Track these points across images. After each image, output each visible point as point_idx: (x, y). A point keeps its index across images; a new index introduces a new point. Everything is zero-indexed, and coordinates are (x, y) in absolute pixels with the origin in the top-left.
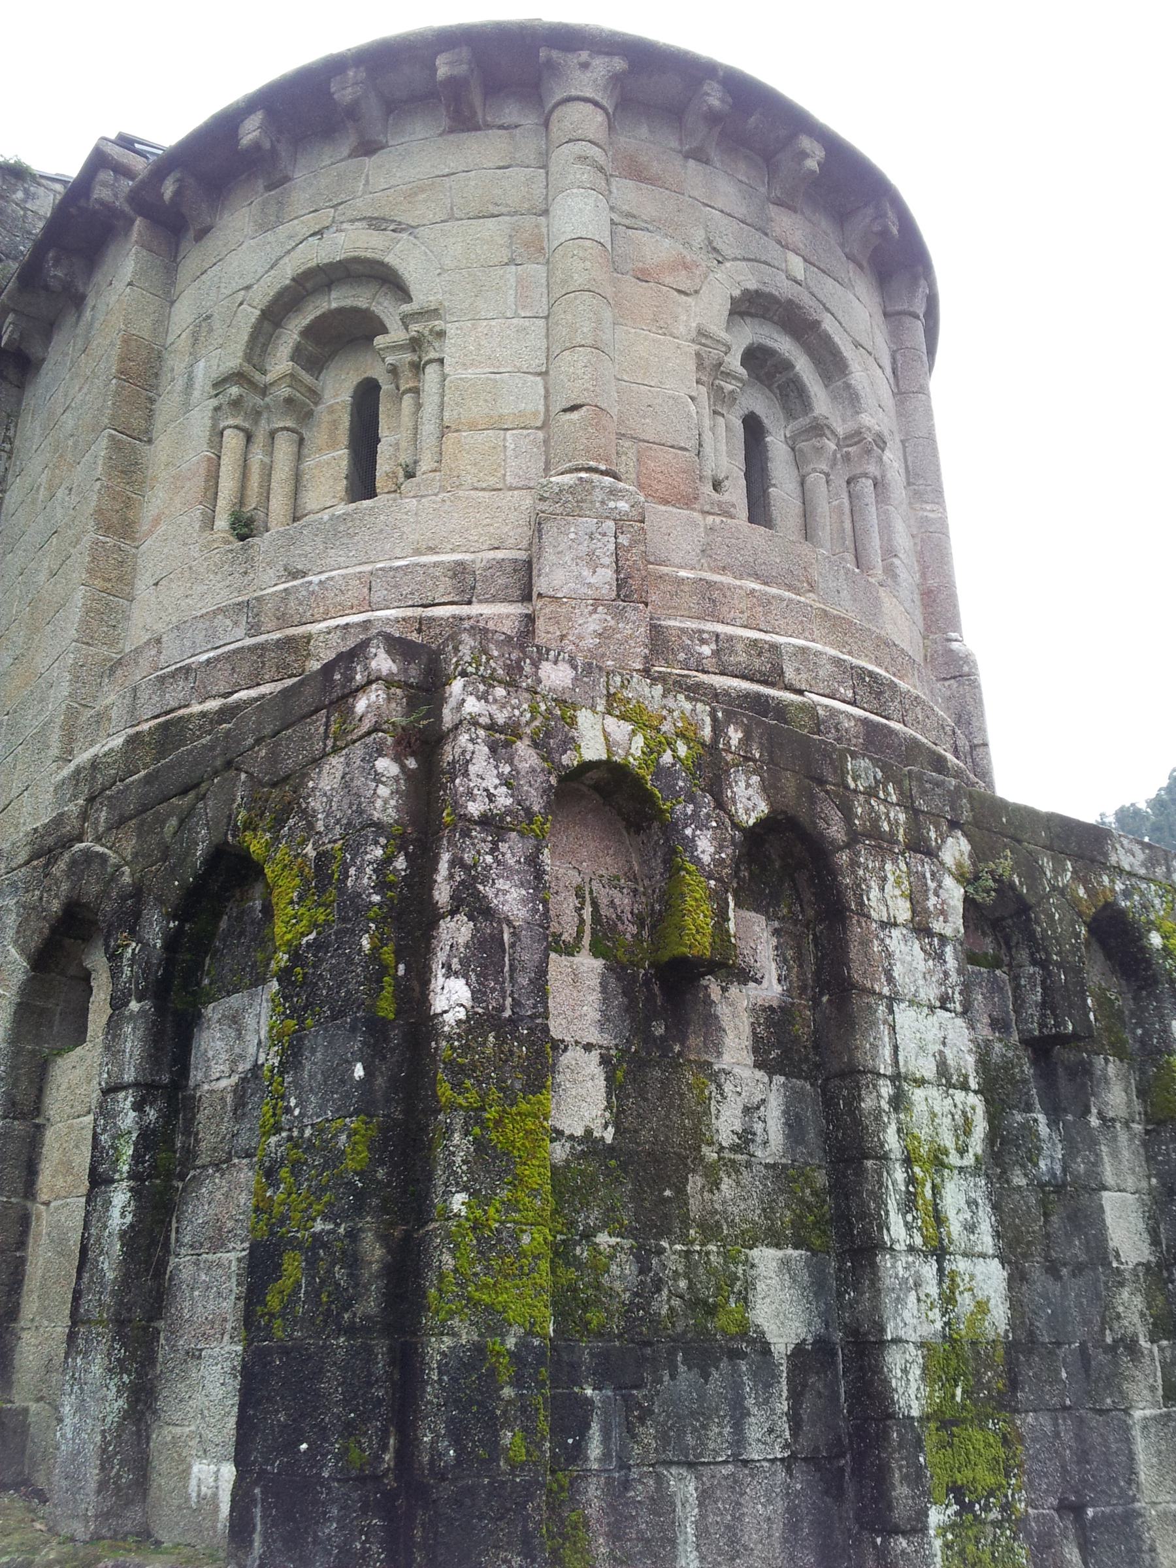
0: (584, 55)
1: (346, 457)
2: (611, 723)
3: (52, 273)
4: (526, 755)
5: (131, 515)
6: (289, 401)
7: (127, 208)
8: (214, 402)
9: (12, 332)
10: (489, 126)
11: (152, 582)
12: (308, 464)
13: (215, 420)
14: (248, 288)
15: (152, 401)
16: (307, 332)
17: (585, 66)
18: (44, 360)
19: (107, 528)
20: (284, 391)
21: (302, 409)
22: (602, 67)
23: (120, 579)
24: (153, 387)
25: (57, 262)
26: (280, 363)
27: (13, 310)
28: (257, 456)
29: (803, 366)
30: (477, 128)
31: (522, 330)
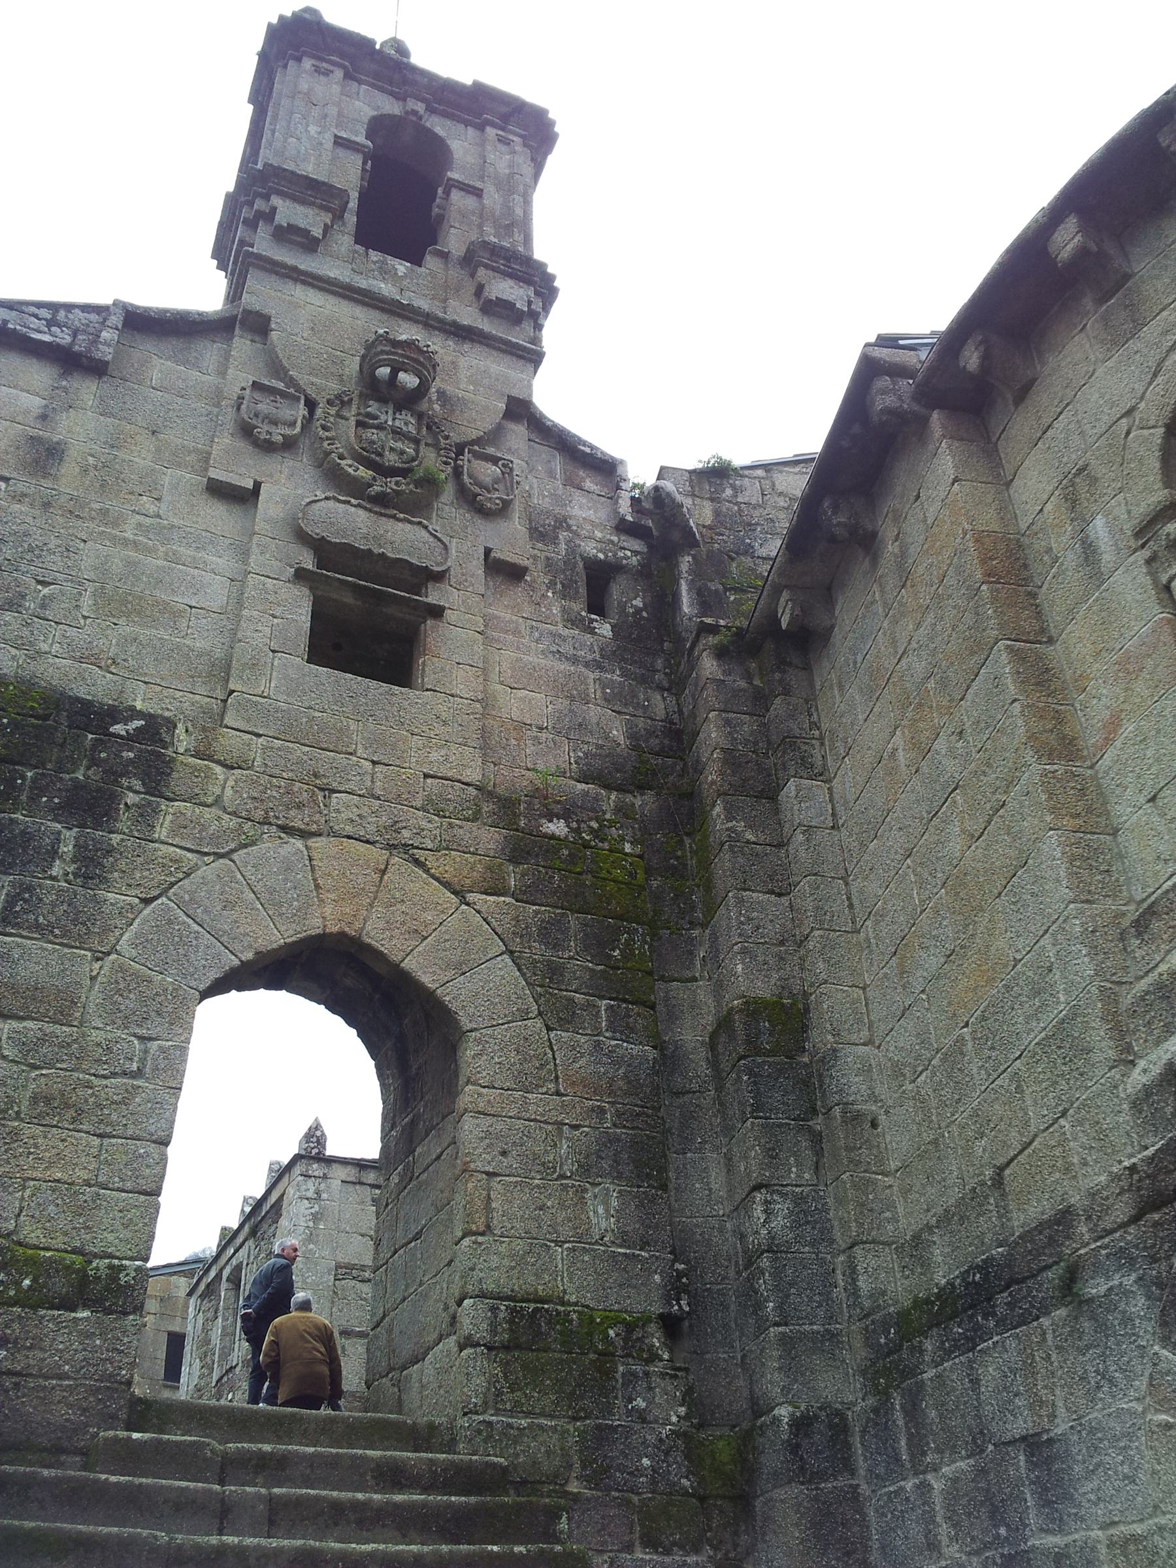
3: (835, 522)
5: (1067, 731)
7: (916, 408)
8: (1146, 553)
9: (793, 609)
11: (1142, 800)
14: (1129, 412)
15: (1034, 595)
18: (833, 627)
19: (1048, 754)
23: (1089, 810)
24: (1027, 581)
25: (836, 508)
27: (786, 587)
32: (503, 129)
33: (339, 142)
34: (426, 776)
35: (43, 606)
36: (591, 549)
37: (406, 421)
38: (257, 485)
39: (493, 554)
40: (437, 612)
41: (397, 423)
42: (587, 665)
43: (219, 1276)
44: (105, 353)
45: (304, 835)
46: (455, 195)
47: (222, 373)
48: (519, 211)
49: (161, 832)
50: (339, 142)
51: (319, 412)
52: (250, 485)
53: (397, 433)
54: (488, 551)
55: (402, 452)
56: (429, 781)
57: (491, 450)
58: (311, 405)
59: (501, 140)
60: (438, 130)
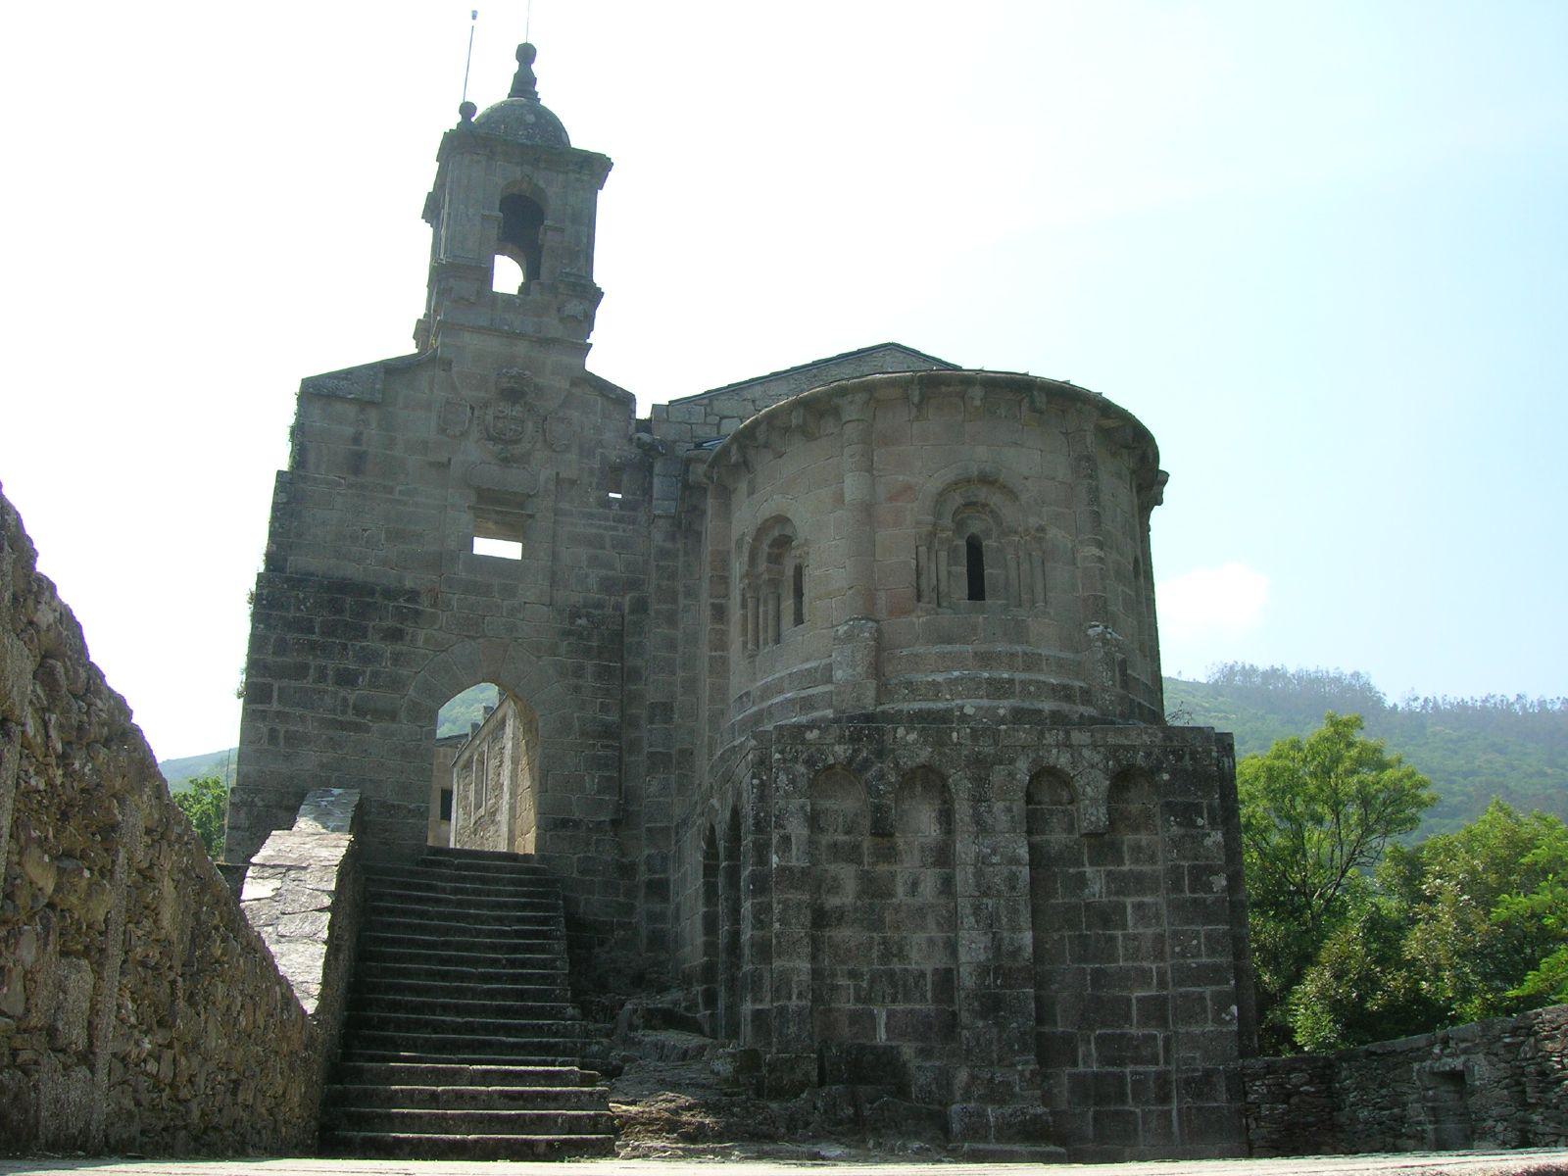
0: (850, 397)
1: (793, 606)
2: (837, 748)
4: (801, 769)
6: (769, 580)
10: (820, 437)
12: (782, 607)
13: (743, 595)
16: (771, 546)
17: (851, 402)
20: (766, 576)
21: (775, 583)
22: (860, 397)
26: (762, 566)
28: (761, 609)
29: (995, 499)
30: (816, 439)
31: (837, 546)
32: (579, 173)
33: (484, 217)
34: (525, 603)
35: (367, 542)
36: (614, 456)
37: (517, 411)
38: (450, 460)
39: (561, 475)
40: (531, 516)
41: (514, 413)
42: (606, 528)
43: (471, 757)
44: (379, 397)
45: (474, 638)
46: (549, 233)
47: (431, 390)
48: (585, 240)
49: (420, 643)
50: (484, 217)
51: (476, 412)
52: (445, 460)
53: (514, 418)
54: (558, 474)
55: (516, 431)
56: (527, 605)
57: (561, 414)
58: (472, 408)
59: (577, 180)
60: (542, 184)
